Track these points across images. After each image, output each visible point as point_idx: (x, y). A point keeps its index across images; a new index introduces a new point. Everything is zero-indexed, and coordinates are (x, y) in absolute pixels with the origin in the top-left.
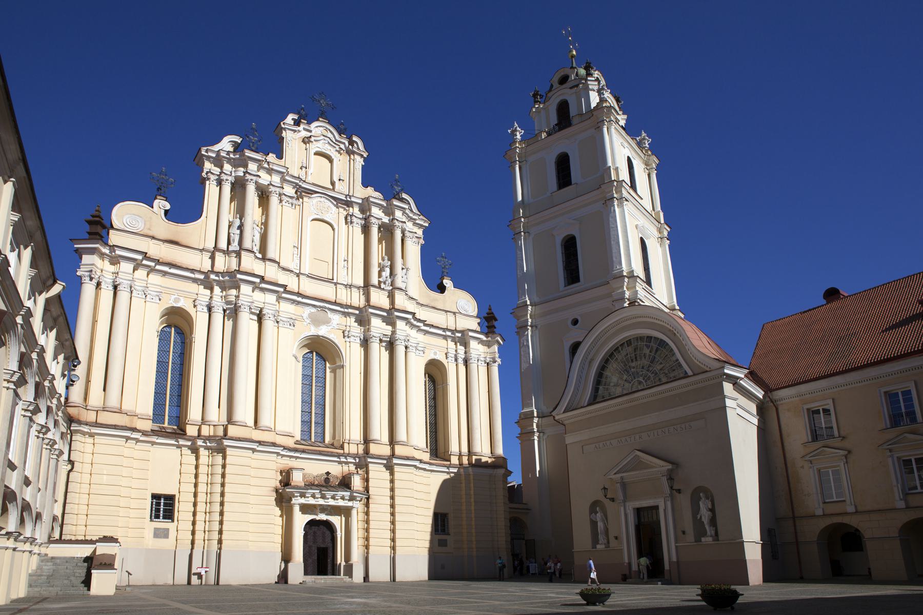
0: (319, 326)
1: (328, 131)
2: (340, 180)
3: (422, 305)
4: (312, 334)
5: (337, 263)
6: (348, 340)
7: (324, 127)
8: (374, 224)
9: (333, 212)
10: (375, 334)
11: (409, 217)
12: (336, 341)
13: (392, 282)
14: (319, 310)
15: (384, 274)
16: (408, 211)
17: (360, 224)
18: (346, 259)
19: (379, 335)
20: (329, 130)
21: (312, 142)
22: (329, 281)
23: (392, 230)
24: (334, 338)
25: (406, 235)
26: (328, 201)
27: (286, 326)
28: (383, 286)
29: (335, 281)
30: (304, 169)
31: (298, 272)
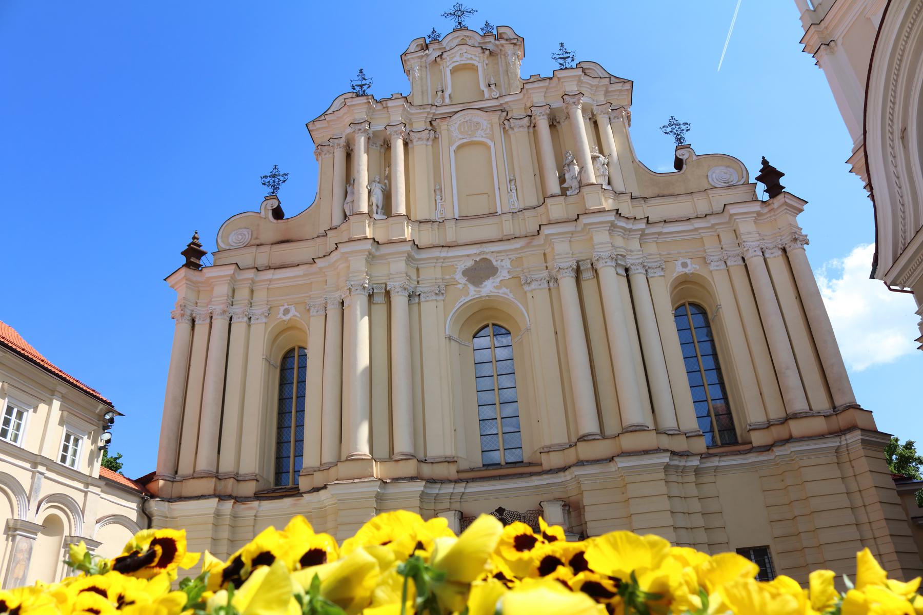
0: (481, 283)
1: (467, 39)
3: (645, 199)
4: (472, 298)
5: (499, 189)
6: (526, 288)
7: (458, 37)
8: (540, 116)
9: (485, 127)
10: (562, 265)
11: (592, 86)
12: (511, 296)
13: (580, 182)
14: (478, 260)
15: (567, 176)
16: (584, 78)
18: (512, 178)
19: (571, 263)
20: (468, 37)
22: (493, 214)
23: (568, 113)
24: (508, 295)
25: (595, 113)
27: (431, 298)
28: (568, 193)
29: (499, 212)
30: (440, 93)
31: (441, 221)
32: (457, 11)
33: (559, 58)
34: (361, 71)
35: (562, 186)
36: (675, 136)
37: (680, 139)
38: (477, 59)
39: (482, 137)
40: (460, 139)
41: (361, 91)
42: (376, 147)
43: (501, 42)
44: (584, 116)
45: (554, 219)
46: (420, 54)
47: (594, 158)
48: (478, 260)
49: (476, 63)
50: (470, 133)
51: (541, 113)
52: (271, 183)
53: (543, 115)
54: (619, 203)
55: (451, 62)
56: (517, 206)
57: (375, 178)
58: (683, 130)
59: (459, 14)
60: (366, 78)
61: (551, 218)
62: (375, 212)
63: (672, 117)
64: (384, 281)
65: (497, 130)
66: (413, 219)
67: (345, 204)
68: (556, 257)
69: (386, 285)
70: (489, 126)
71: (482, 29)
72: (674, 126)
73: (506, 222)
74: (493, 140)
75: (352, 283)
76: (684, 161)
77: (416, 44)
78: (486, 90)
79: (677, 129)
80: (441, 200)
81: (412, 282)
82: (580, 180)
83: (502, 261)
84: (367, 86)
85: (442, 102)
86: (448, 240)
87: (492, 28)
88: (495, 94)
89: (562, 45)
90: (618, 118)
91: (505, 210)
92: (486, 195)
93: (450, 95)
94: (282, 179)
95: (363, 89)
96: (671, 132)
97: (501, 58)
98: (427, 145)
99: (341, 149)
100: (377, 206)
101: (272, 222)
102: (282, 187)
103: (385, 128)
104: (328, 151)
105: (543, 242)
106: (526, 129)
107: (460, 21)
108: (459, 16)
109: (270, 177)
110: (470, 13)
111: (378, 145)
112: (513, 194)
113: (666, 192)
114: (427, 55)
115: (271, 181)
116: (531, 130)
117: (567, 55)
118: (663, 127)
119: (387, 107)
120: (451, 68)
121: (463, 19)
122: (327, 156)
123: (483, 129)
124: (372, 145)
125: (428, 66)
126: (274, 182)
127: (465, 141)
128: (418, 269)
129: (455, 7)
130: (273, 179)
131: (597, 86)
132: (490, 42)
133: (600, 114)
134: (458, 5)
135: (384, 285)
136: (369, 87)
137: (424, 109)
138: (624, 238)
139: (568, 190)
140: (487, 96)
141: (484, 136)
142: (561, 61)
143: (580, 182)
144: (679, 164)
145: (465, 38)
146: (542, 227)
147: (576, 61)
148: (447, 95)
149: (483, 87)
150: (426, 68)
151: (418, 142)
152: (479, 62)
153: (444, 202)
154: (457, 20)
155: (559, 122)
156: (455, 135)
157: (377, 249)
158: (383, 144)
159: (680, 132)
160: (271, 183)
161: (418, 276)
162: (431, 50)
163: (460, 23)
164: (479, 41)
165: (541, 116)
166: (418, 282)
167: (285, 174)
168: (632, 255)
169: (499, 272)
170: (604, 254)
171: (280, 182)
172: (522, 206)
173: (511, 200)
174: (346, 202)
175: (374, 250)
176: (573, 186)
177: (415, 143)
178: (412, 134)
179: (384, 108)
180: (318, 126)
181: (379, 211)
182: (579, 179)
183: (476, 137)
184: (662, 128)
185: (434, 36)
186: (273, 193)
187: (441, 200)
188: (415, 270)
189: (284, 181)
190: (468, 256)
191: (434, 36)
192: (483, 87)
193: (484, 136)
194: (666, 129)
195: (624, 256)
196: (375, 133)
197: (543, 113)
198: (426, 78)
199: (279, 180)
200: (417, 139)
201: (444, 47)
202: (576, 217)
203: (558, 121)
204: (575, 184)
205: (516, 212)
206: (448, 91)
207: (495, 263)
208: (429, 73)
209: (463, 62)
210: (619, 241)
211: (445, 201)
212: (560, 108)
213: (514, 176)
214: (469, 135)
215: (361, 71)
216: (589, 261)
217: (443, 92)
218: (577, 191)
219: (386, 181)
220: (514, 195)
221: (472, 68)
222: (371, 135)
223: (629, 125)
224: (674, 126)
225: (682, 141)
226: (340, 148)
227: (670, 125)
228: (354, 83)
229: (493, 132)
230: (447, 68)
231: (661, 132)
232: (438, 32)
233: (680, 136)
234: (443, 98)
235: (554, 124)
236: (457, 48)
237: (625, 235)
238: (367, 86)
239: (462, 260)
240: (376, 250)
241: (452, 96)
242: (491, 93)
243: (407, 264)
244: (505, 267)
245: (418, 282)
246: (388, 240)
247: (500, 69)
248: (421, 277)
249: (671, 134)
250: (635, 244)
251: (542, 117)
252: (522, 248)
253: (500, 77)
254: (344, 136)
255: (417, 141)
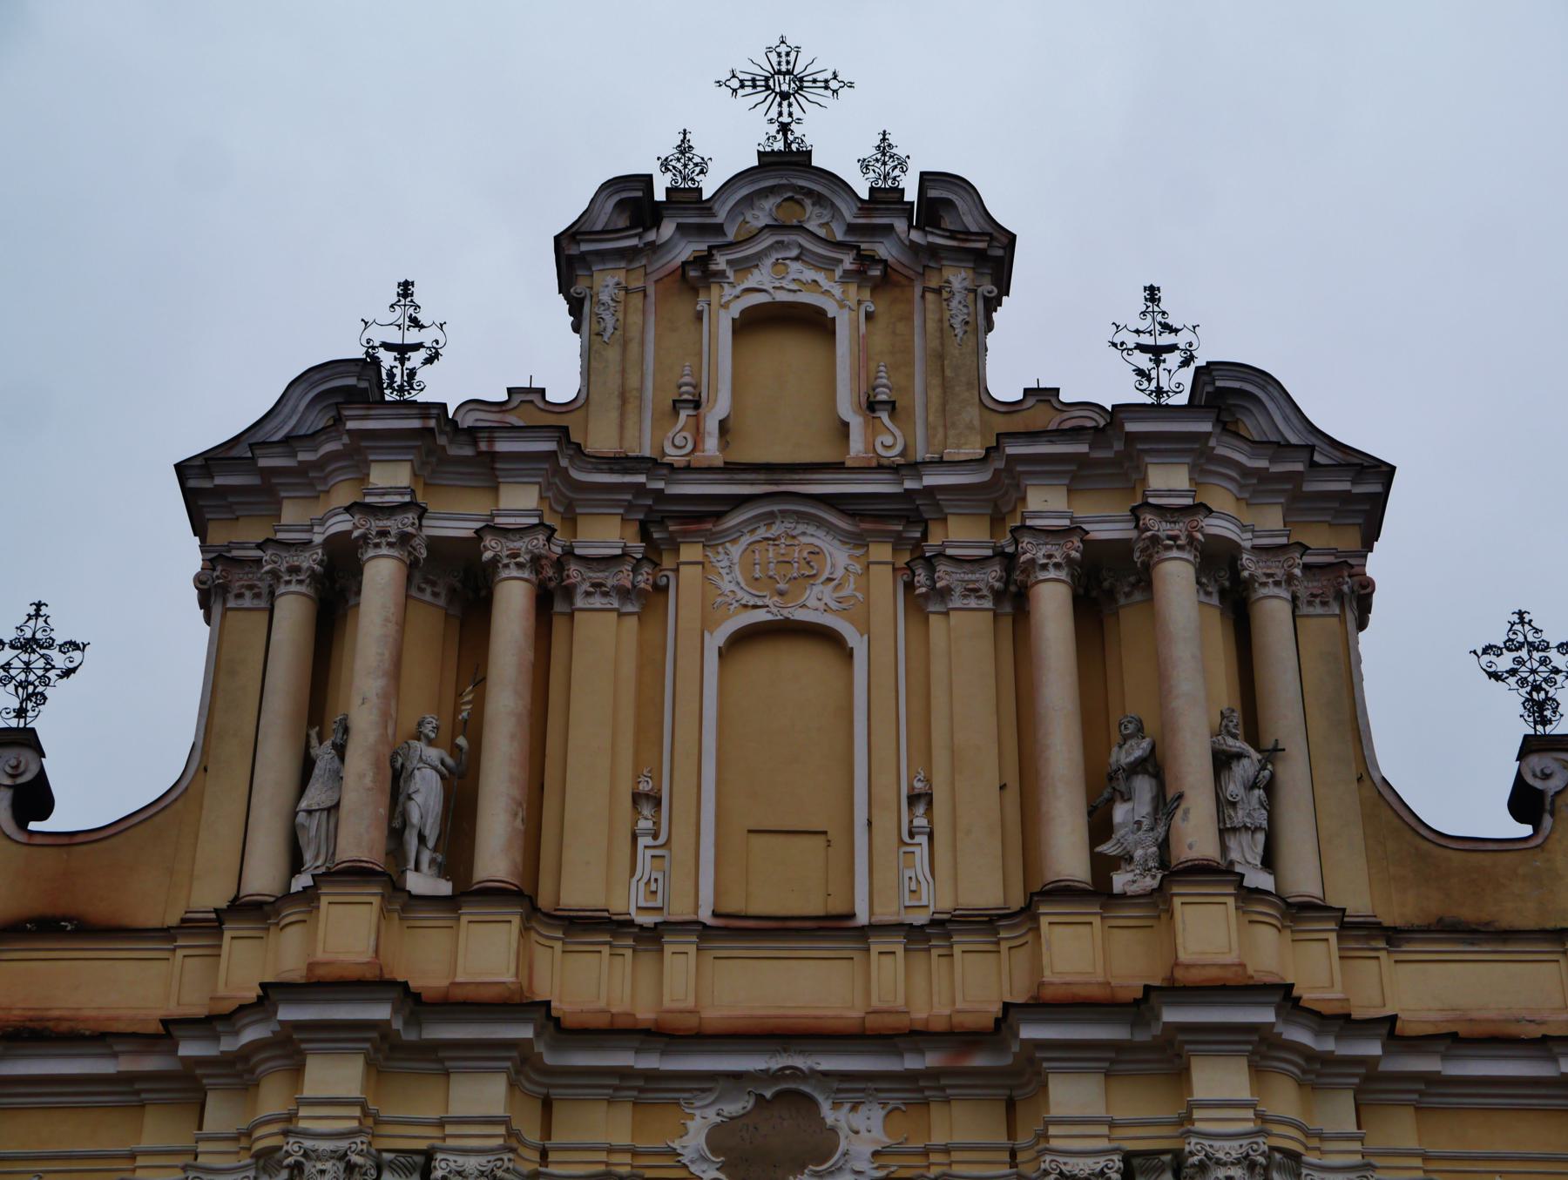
1: (808, 202)
2: (872, 406)
5: (870, 823)
7: (771, 191)
8: (1044, 567)
9: (839, 574)
11: (1246, 472)
14: (768, 1094)
15: (1120, 813)
17: (985, 592)
19: (1101, 1162)
20: (810, 193)
21: (722, 274)
26: (811, 530)
28: (1120, 881)
29: (862, 918)
31: (647, 920)
32: (779, 72)
33: (1143, 348)
34: (406, 288)
35: (1099, 849)
36: (1523, 691)
37: (1541, 706)
38: (837, 291)
39: (827, 609)
40: (745, 606)
41: (397, 372)
42: (435, 595)
43: (931, 239)
44: (1204, 580)
45: (1056, 979)
46: (634, 242)
47: (1222, 761)
48: (768, 1094)
49: (832, 310)
50: (782, 586)
51: (1050, 556)
52: (12, 672)
53: (1057, 566)
54: (1293, 941)
55: (738, 290)
56: (935, 899)
57: (420, 724)
58: (1556, 671)
59: (785, 88)
60: (422, 317)
61: (1048, 976)
62: (412, 865)
63: (1521, 614)
64: (422, 1145)
65: (883, 583)
66: (545, 901)
67: (301, 817)
68: (1052, 1130)
69: (429, 1155)
70: (858, 568)
71: (865, 165)
72: (1525, 650)
73: (883, 958)
74: (865, 629)
75: (308, 1144)
76: (1548, 800)
77: (616, 198)
78: (856, 423)
79: (1536, 665)
80: (655, 836)
81: (522, 1150)
82: (1166, 839)
83: (854, 1108)
84: (422, 354)
85: (690, 447)
86: (667, 1003)
87: (902, 164)
88: (890, 444)
89: (1152, 294)
90: (1324, 604)
91: (888, 913)
92: (820, 840)
93: (721, 422)
94: (59, 660)
95: (408, 365)
96: (1513, 672)
97: (923, 297)
98: (621, 615)
99: (303, 589)
100: (422, 839)
101: (9, 837)
102: (58, 692)
103: (477, 531)
104: (250, 587)
105: (1006, 1061)
106: (988, 604)
107: (785, 119)
108: (785, 96)
109: (13, 647)
110: (826, 88)
111: (441, 589)
112: (917, 850)
113: (1467, 913)
114: (653, 248)
115: (16, 663)
116: (1007, 608)
117: (1166, 339)
118: (1486, 650)
119: (494, 456)
120: (737, 316)
121: (795, 109)
122: (247, 602)
123: (832, 580)
124: (421, 590)
125: (651, 290)
126: (27, 667)
127: (761, 616)
128: (547, 1105)
129: (774, 57)
130: (25, 657)
131: (1262, 476)
132: (890, 228)
133: (1264, 584)
134: (783, 49)
135: (419, 1159)
136: (429, 360)
137: (625, 471)
138: (1301, 1085)
139: (1117, 868)
140: (857, 446)
141: (834, 605)
142: (1144, 360)
143: (1164, 845)
144: (1524, 802)
145: (797, 197)
146: (1012, 1011)
147: (1200, 361)
148: (711, 425)
149: (846, 408)
150: (645, 296)
151: (591, 600)
152: (842, 305)
153: (666, 845)
154: (773, 113)
155: (1111, 595)
156: (727, 587)
157: (414, 1020)
158: (458, 585)
159: (1545, 680)
160: (12, 672)
161: (547, 1131)
162: (668, 229)
163: (784, 128)
164: (850, 219)
165: (1051, 568)
166: (544, 1154)
167: (74, 646)
168: (1323, 1152)
169: (843, 1146)
170: (1227, 1144)
171: (52, 674)
172: (946, 903)
173: (908, 873)
174: (303, 804)
175: (397, 1025)
176: (1138, 853)
177: (580, 602)
178: (573, 569)
179: (480, 454)
180: (219, 481)
181: (425, 865)
182: (1161, 830)
183: (804, 606)
184: (1479, 652)
185: (685, 166)
186: (21, 713)
187: (655, 836)
188: (537, 1107)
189: (67, 673)
190: (737, 1076)
191: (685, 166)
192: (846, 408)
193: (834, 605)
194: (1493, 658)
195: (1294, 1156)
196: (434, 543)
197: (1058, 560)
198: (642, 343)
199: (49, 666)
200: (586, 587)
201: (719, 220)
202: (1140, 995)
203: (1106, 584)
204: (1145, 851)
205: (922, 926)
206: (719, 407)
207: (829, 1114)
208: (652, 319)
209: (782, 296)
210: (1284, 1100)
211: (666, 845)
212: (1121, 548)
213: (928, 780)
214: (781, 594)
215: (406, 288)
216: (1167, 1158)
217: (697, 404)
218: (1150, 883)
219: (461, 741)
220: (921, 853)
221: (815, 323)
222: (424, 553)
223: (1362, 624)
224: (1524, 653)
225: (1548, 713)
226: (300, 582)
227: (1511, 645)
228: (378, 335)
229: (867, 592)
230: (722, 313)
231: (1473, 670)
232: (700, 150)
233: (1542, 695)
234: (698, 434)
235: (1094, 594)
236: (768, 241)
237: (1304, 1072)
238: (422, 354)
239: (710, 1090)
240: (406, 1023)
241: (731, 423)
242: (875, 434)
243: (512, 1085)
244: (863, 1133)
245: (544, 1154)
246: (454, 984)
247: (918, 340)
248: (558, 1138)
249: (1512, 680)
250: (1339, 1113)
251: (1052, 574)
252: (932, 1074)
253: (911, 376)
254: (318, 539)
255: (588, 594)
